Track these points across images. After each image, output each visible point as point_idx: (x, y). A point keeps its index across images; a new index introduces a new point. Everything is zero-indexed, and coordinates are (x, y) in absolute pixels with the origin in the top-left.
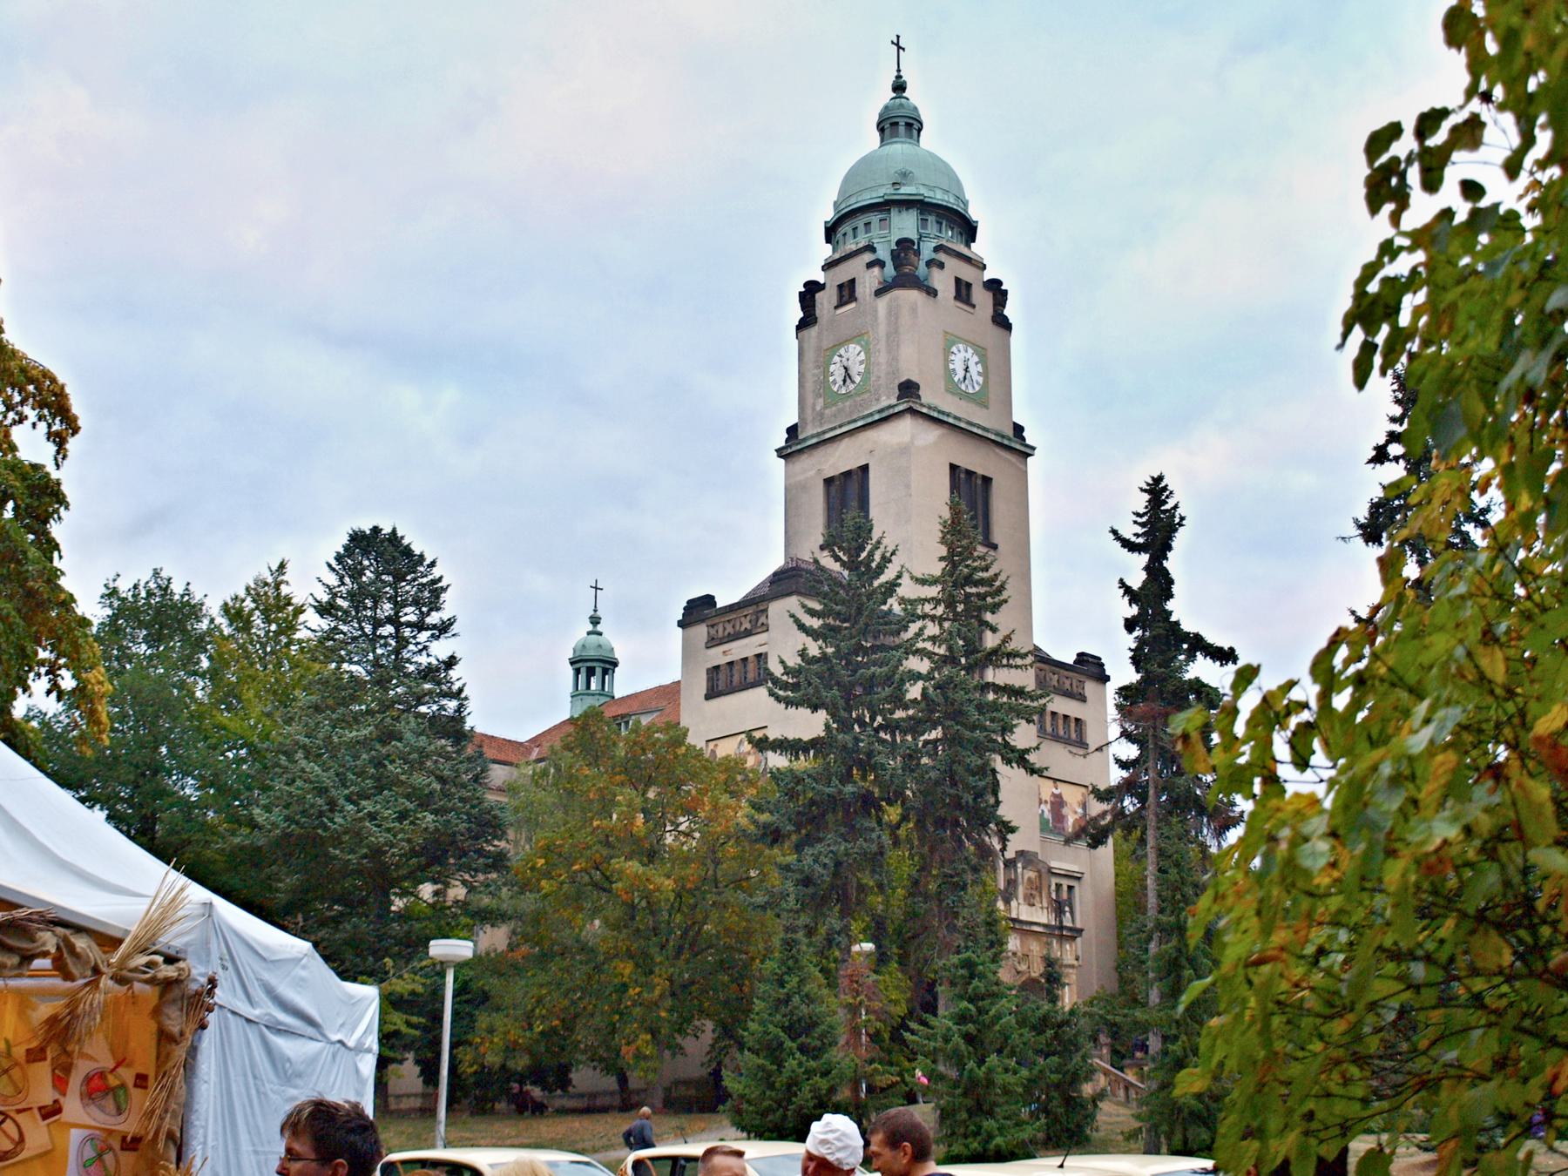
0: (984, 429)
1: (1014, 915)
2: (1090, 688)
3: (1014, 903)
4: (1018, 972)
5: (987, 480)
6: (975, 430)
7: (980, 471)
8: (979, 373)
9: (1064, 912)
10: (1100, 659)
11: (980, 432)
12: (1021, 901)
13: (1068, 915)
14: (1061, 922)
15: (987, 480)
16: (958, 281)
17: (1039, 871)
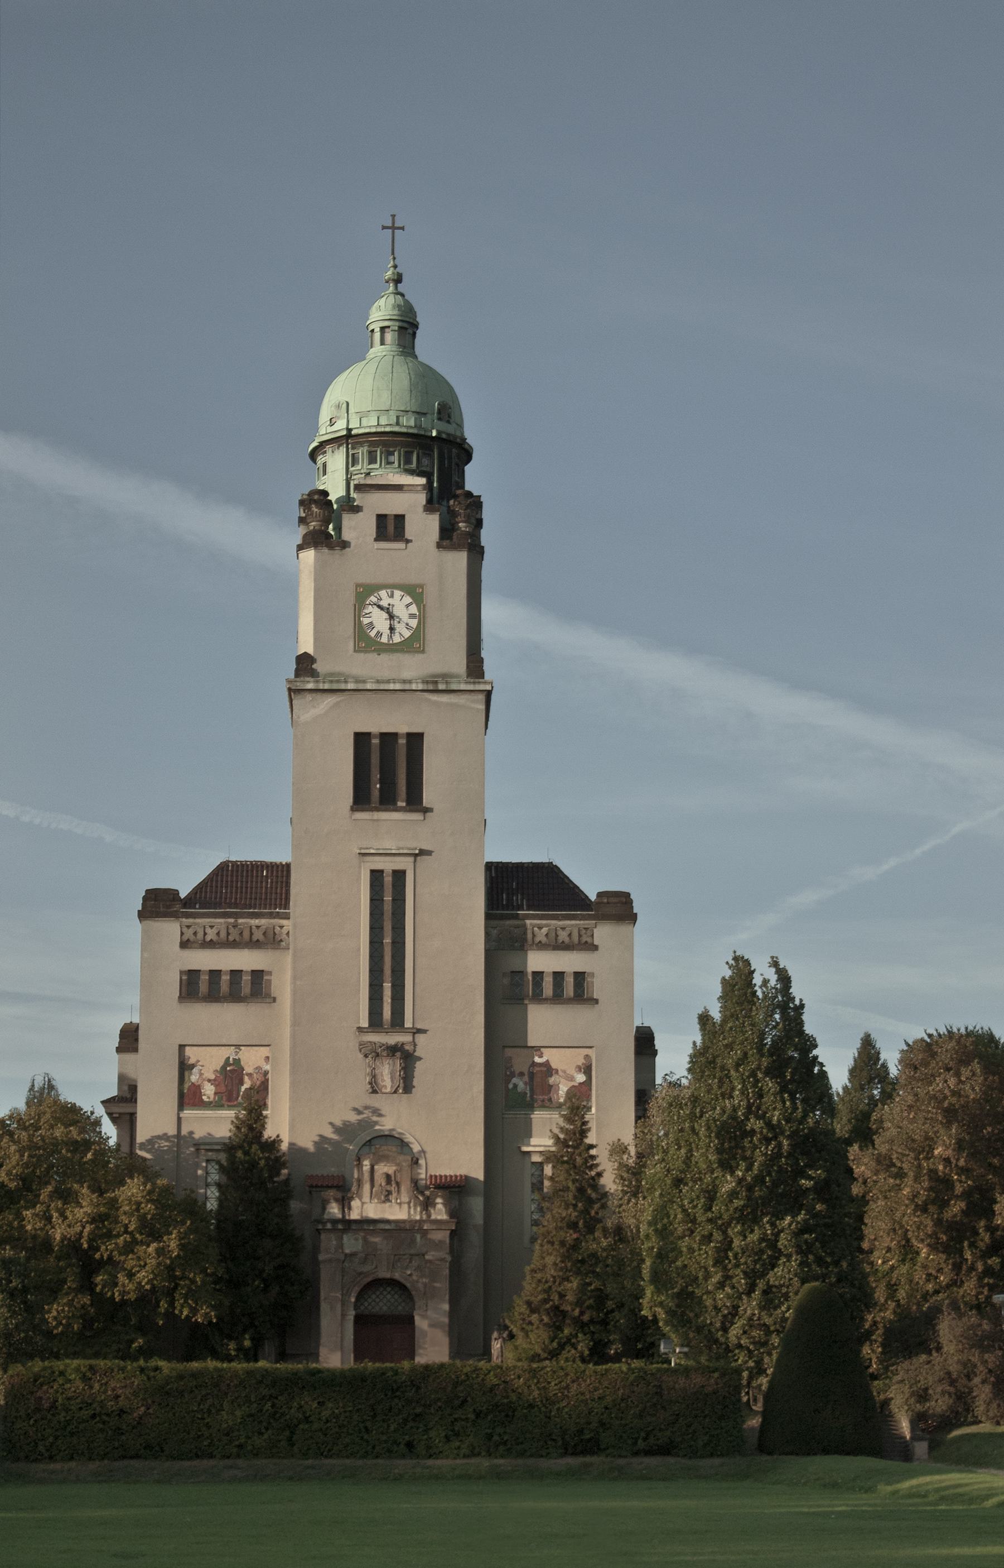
0: (404, 682)
1: (354, 1215)
2: (603, 933)
3: (355, 1204)
4: (360, 1274)
5: (415, 740)
6: (391, 686)
7: (403, 729)
8: (412, 616)
9: (434, 1205)
10: (628, 895)
11: (398, 686)
12: (366, 1198)
13: (440, 1206)
14: (429, 1216)
15: (415, 740)
16: (381, 519)
17: (398, 1165)
